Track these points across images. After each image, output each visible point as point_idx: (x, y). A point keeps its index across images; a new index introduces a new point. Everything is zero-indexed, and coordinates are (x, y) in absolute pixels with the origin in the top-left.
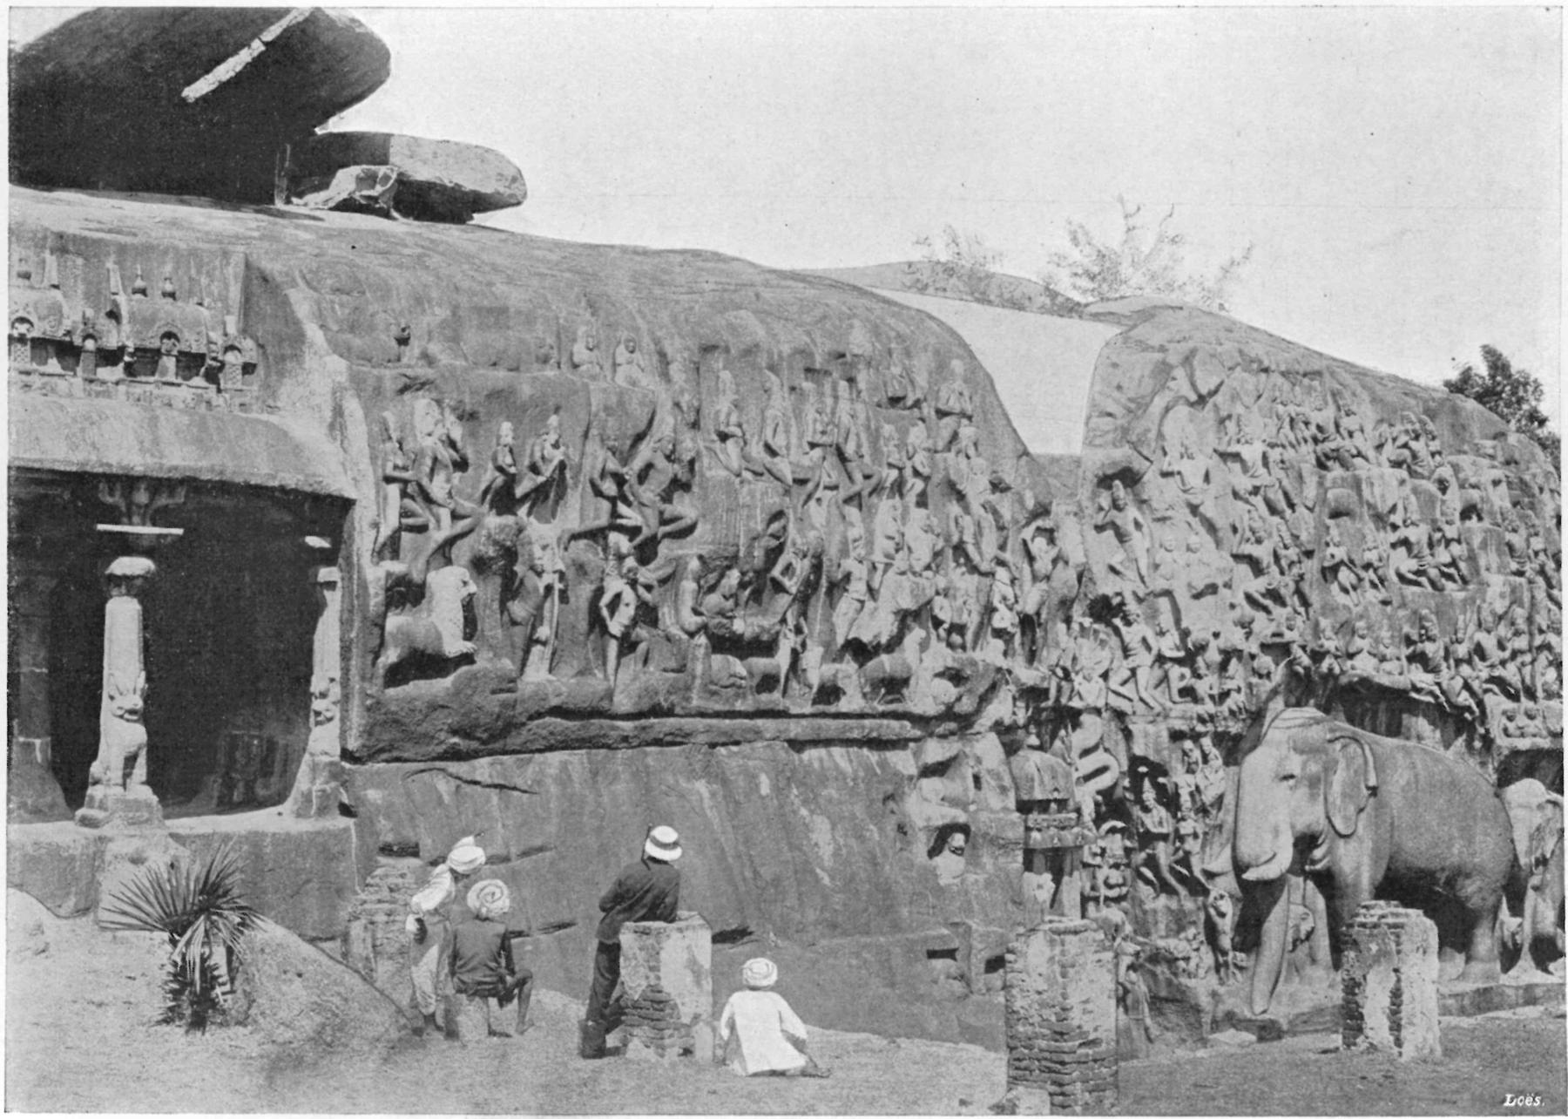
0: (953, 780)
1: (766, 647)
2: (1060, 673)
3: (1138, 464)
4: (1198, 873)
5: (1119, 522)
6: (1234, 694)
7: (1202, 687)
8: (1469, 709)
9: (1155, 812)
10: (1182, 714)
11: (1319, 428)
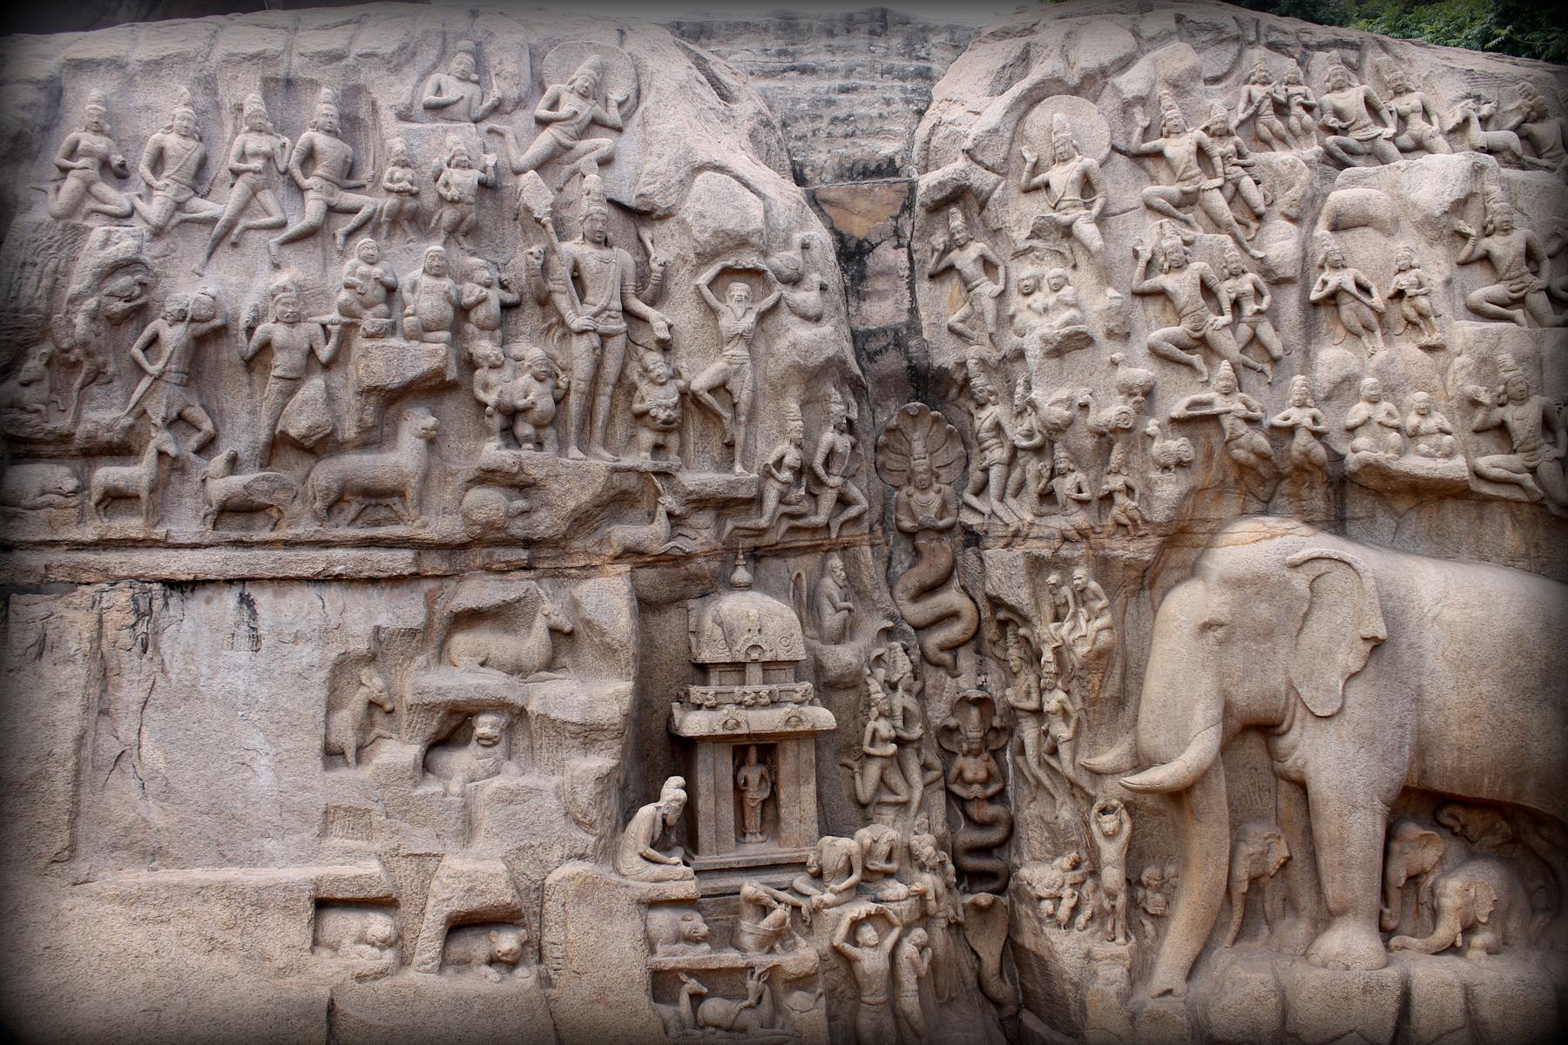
0: (515, 631)
1: (122, 450)
2: (786, 475)
3: (981, 179)
4: (1068, 770)
5: (958, 266)
6: (1120, 499)
7: (1065, 486)
9: (1022, 677)
11: (1338, 113)
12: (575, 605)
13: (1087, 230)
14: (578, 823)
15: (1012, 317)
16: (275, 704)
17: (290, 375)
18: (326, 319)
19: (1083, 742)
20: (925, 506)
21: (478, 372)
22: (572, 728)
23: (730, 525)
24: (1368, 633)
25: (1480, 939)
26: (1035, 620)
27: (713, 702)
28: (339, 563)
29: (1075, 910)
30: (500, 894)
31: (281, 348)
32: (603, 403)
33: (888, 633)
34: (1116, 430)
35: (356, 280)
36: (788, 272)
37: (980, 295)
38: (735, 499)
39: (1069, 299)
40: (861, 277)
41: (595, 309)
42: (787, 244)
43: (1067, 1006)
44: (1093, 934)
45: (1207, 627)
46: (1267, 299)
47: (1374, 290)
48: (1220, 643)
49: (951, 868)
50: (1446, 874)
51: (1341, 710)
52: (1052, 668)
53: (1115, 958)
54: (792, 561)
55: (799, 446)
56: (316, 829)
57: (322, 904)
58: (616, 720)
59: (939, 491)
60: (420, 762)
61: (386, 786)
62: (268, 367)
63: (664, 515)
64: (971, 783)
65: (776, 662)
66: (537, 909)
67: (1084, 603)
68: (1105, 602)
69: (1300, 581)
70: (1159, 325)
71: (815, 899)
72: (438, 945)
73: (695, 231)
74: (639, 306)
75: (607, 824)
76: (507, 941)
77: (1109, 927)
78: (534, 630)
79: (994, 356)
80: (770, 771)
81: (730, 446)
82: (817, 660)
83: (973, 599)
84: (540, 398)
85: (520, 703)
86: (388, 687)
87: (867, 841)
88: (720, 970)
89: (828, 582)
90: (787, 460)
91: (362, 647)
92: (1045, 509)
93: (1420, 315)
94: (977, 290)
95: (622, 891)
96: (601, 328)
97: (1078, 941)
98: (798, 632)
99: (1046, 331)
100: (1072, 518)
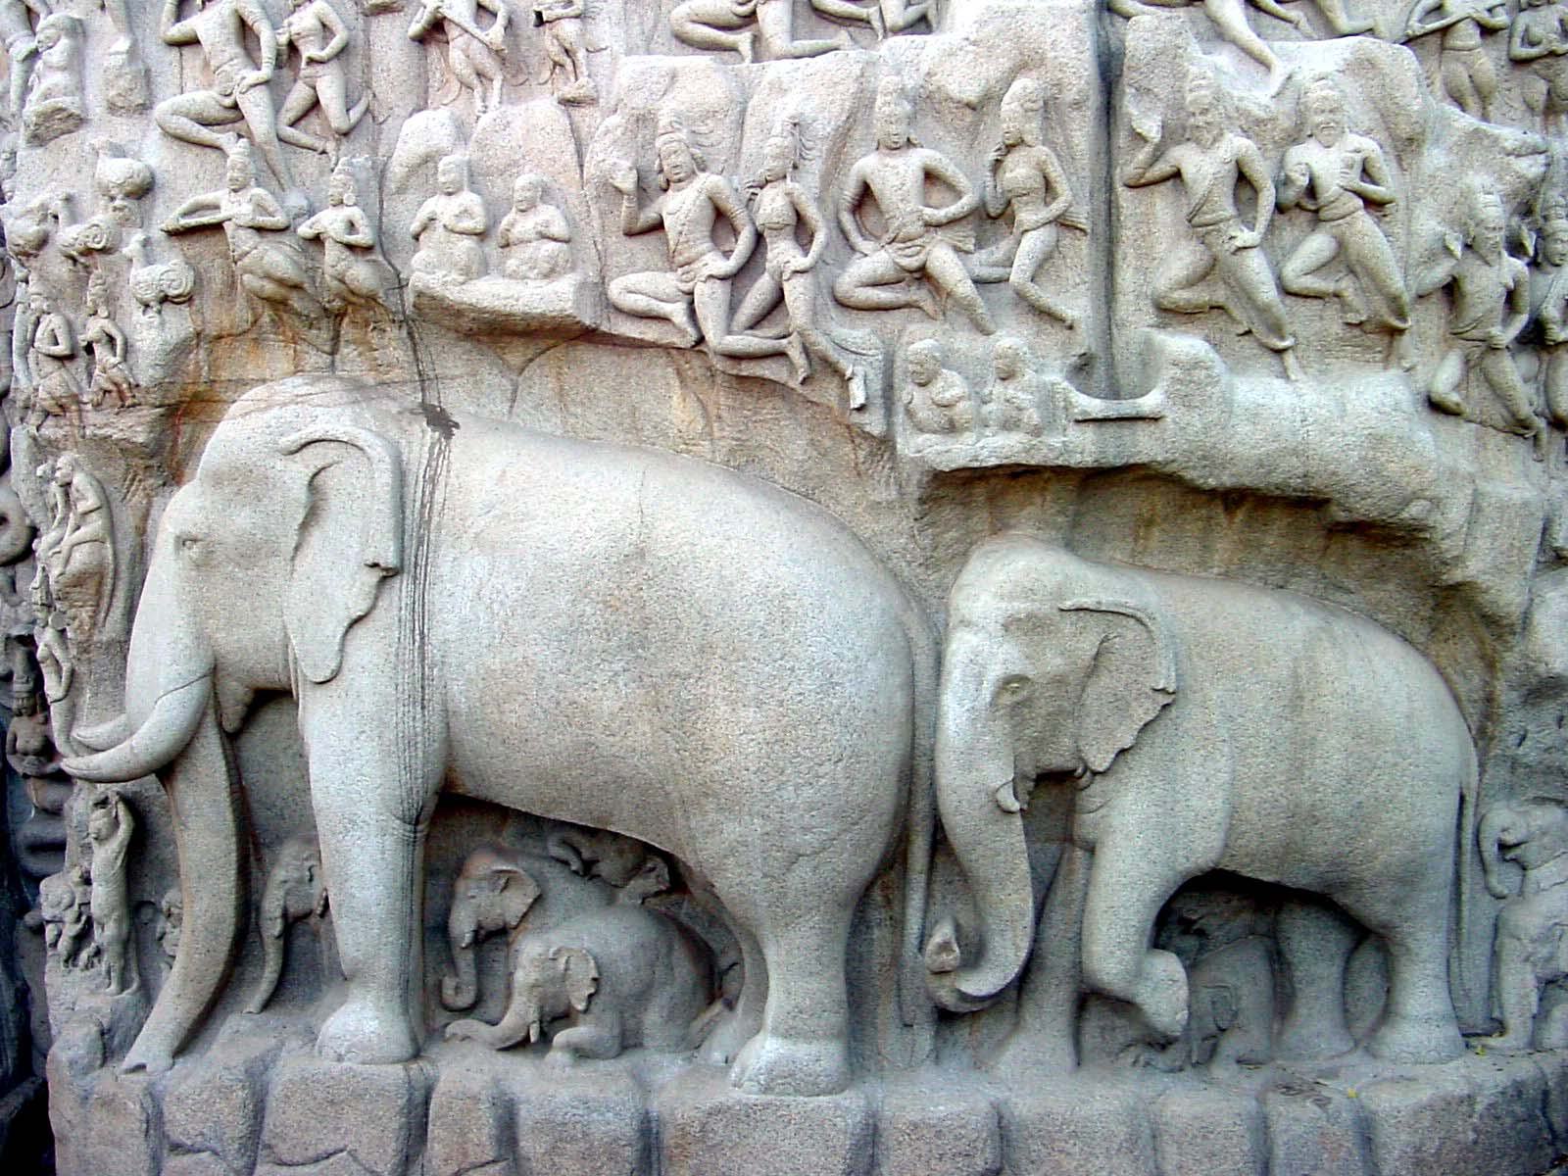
8: (780, 354)
25: (561, 1037)
26: (43, 528)
29: (83, 937)
34: (88, 252)
44: (92, 978)
50: (543, 928)
52: (38, 597)
64: (26, 754)
68: (90, 501)
69: (297, 472)
77: (103, 967)
93: (567, 51)
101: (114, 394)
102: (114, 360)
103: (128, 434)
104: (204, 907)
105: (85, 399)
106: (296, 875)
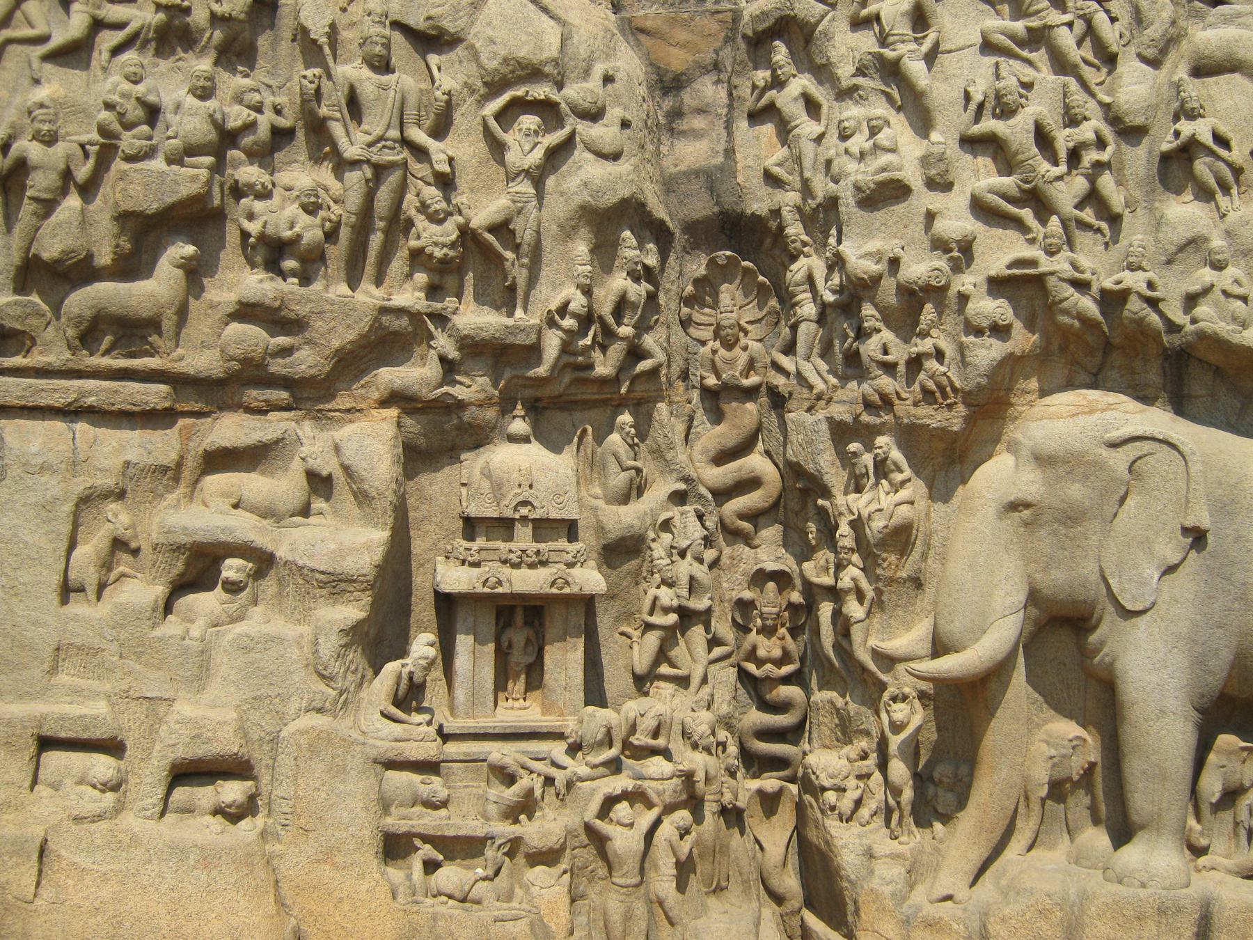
0: (272, 474)
10: (846, 401)
12: (337, 449)
13: (916, 68)
14: (322, 676)
15: (829, 163)
16: (16, 536)
17: (44, 196)
18: (84, 138)
19: (876, 620)
20: (731, 363)
21: (243, 201)
22: (318, 576)
23: (508, 374)
24: (1189, 523)
26: (834, 491)
27: (476, 558)
28: (90, 393)
29: (858, 803)
30: (226, 743)
31: (35, 168)
32: (376, 240)
33: (679, 498)
35: (116, 98)
36: (586, 105)
37: (799, 136)
38: (513, 346)
39: (886, 143)
40: (677, 114)
41: (369, 138)
42: (586, 73)
43: (845, 904)
45: (1014, 506)
46: (1110, 149)
47: (1233, 144)
48: (1026, 524)
49: (733, 749)
51: (1153, 604)
52: (848, 542)
53: (895, 856)
54: (578, 415)
55: (587, 292)
56: (46, 666)
57: (46, 743)
58: (365, 572)
59: (745, 349)
60: (161, 603)
61: (122, 626)
62: (24, 187)
63: (436, 359)
65: (548, 520)
66: (270, 762)
67: (886, 477)
68: (908, 473)
69: (1119, 460)
70: (988, 173)
71: (568, 772)
72: (160, 791)
73: (486, 62)
74: (419, 136)
75: (350, 677)
76: (232, 791)
78: (290, 473)
79: (812, 203)
80: (537, 633)
81: (512, 289)
82: (599, 521)
83: (776, 465)
84: (309, 230)
85: (270, 547)
86: (133, 526)
87: (632, 715)
88: (457, 838)
89: (615, 438)
90: (572, 307)
91: (109, 482)
92: (850, 372)
94: (796, 131)
95: (358, 749)
96: (375, 159)
97: (860, 837)
98: (572, 490)
99: (860, 177)
100: (876, 382)
101: (938, 395)
102: (943, 369)
103: (945, 424)
104: (1003, 775)
105: (904, 395)
106: (1064, 751)
